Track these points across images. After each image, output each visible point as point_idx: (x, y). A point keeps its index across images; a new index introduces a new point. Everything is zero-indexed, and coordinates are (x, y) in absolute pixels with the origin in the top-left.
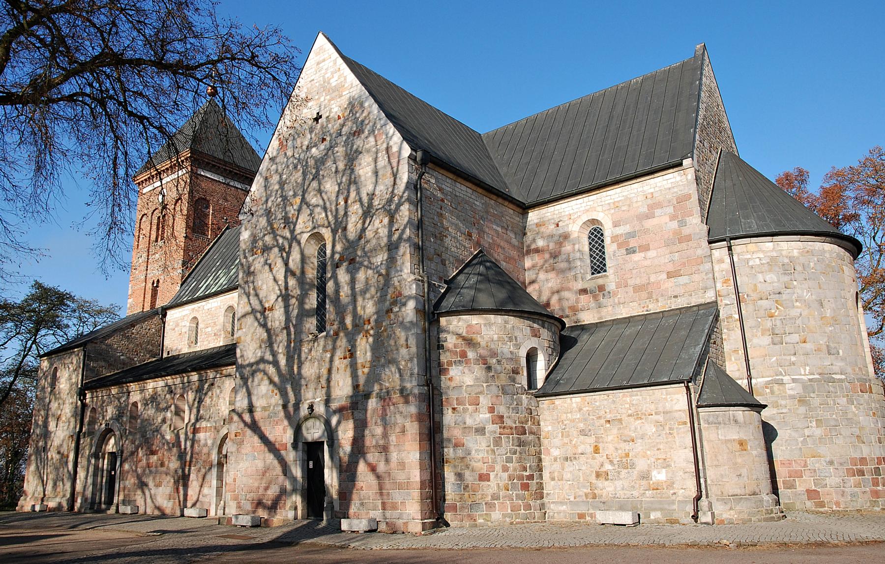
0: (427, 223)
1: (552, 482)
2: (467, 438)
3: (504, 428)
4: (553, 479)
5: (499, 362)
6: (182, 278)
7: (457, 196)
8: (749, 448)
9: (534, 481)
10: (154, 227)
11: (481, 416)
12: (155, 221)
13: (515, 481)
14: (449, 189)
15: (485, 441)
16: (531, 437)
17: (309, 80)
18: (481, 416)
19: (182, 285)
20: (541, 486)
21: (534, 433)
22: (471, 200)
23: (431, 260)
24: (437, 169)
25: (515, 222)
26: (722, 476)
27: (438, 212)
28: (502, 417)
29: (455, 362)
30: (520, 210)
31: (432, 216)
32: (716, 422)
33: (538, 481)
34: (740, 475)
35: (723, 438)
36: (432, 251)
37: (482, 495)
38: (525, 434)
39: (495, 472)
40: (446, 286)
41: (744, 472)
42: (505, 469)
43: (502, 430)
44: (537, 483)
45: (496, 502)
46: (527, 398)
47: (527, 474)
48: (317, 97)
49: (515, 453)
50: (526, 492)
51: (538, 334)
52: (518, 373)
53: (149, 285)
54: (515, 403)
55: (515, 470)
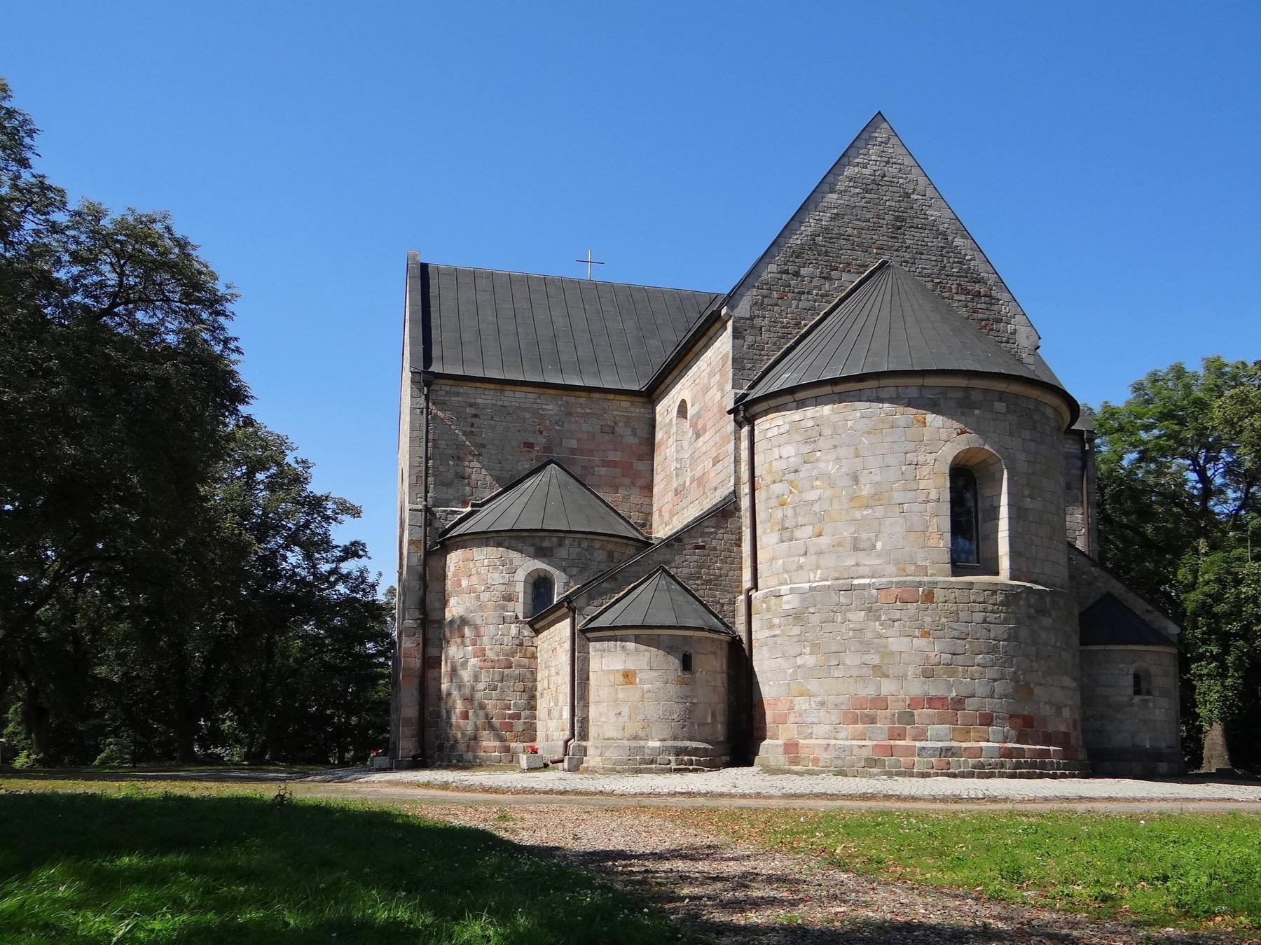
21: (524, 667)
30: (644, 400)
44: (525, 723)
47: (511, 712)
49: (495, 688)
52: (510, 599)
54: (500, 633)
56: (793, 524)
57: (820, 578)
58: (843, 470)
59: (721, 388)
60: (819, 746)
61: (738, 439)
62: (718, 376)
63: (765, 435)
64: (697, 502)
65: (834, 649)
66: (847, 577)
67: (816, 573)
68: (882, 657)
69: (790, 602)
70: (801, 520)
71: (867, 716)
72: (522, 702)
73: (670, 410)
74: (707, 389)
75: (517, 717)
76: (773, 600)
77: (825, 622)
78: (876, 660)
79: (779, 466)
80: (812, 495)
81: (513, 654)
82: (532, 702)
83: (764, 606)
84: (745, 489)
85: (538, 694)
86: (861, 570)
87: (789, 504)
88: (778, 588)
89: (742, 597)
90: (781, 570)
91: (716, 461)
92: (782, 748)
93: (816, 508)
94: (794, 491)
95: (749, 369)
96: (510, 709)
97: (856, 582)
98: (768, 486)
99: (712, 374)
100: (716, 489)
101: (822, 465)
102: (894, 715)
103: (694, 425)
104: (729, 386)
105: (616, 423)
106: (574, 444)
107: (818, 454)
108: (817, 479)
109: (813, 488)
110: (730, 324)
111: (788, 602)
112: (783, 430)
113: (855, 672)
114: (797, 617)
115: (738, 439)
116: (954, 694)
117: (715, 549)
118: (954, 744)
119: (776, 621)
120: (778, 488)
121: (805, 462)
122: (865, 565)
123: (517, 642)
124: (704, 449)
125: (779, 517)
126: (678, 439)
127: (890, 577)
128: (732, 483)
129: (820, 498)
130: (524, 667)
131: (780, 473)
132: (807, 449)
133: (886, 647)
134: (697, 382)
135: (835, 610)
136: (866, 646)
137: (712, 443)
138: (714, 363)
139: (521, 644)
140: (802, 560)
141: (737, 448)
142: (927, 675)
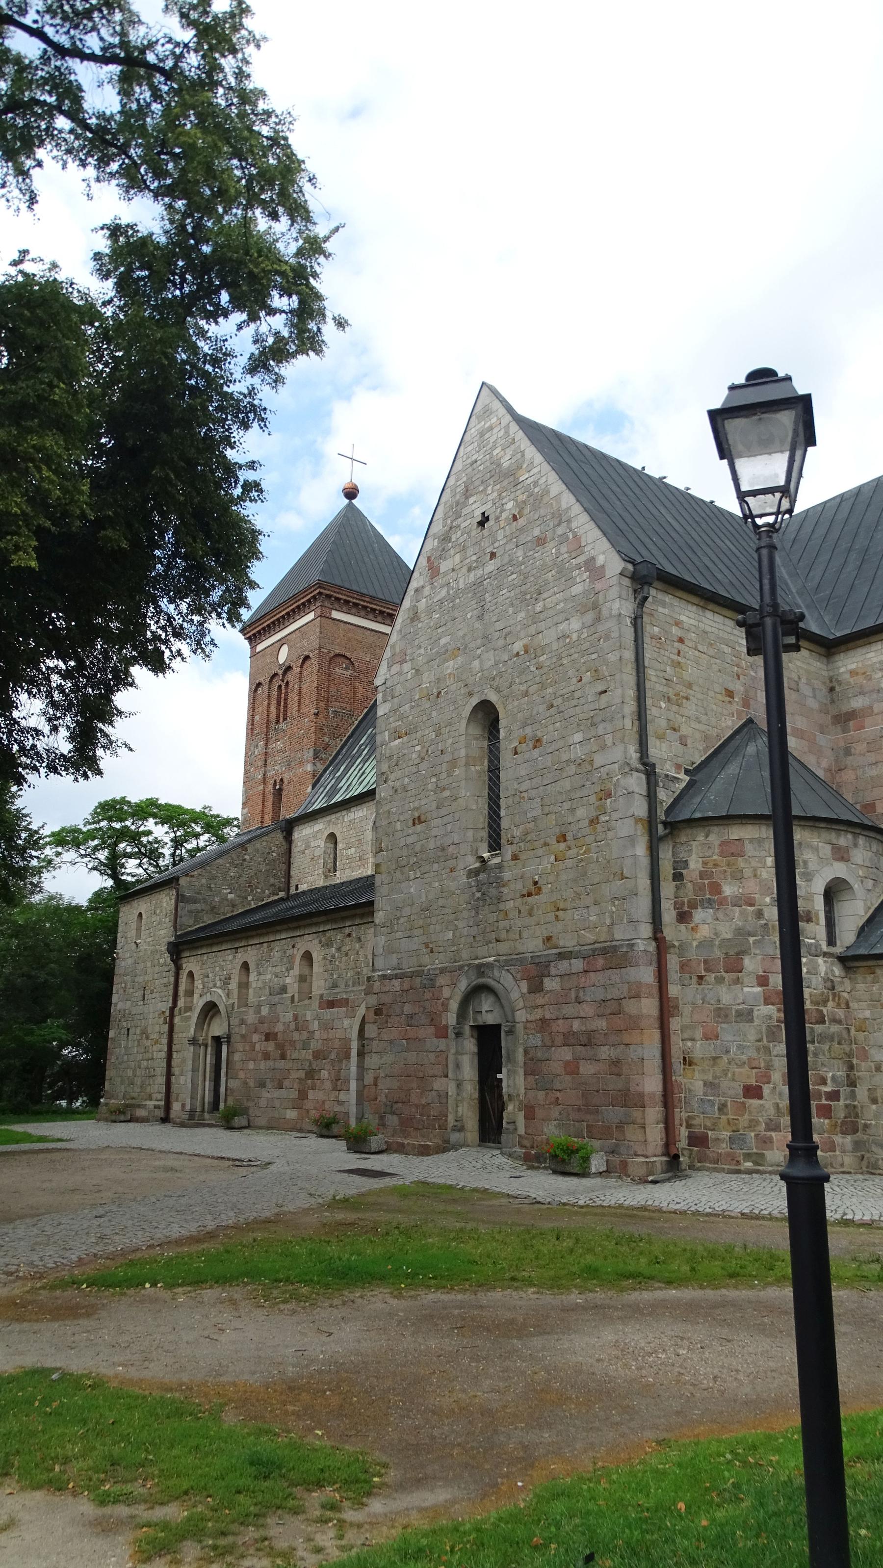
0: (653, 679)
1: (874, 1107)
2: (723, 1025)
4: (874, 1101)
6: (314, 776)
7: (707, 633)
9: (842, 1102)
10: (274, 702)
11: (745, 989)
12: (275, 693)
14: (692, 622)
15: (753, 1031)
16: (835, 1028)
17: (469, 461)
19: (313, 788)
20: (853, 1111)
21: (839, 1022)
22: (732, 638)
23: (661, 737)
24: (671, 589)
25: (813, 669)
27: (673, 661)
29: (702, 901)
30: (822, 650)
31: (662, 667)
33: (848, 1102)
36: (663, 723)
37: (751, 1121)
38: (823, 1022)
40: (687, 778)
44: (847, 1106)
45: (773, 1134)
46: (825, 962)
47: (828, 1089)
48: (481, 488)
50: (827, 1121)
51: (845, 856)
53: (270, 787)
72: (841, 1074)
81: (825, 1002)
123: (829, 984)
130: (839, 1022)
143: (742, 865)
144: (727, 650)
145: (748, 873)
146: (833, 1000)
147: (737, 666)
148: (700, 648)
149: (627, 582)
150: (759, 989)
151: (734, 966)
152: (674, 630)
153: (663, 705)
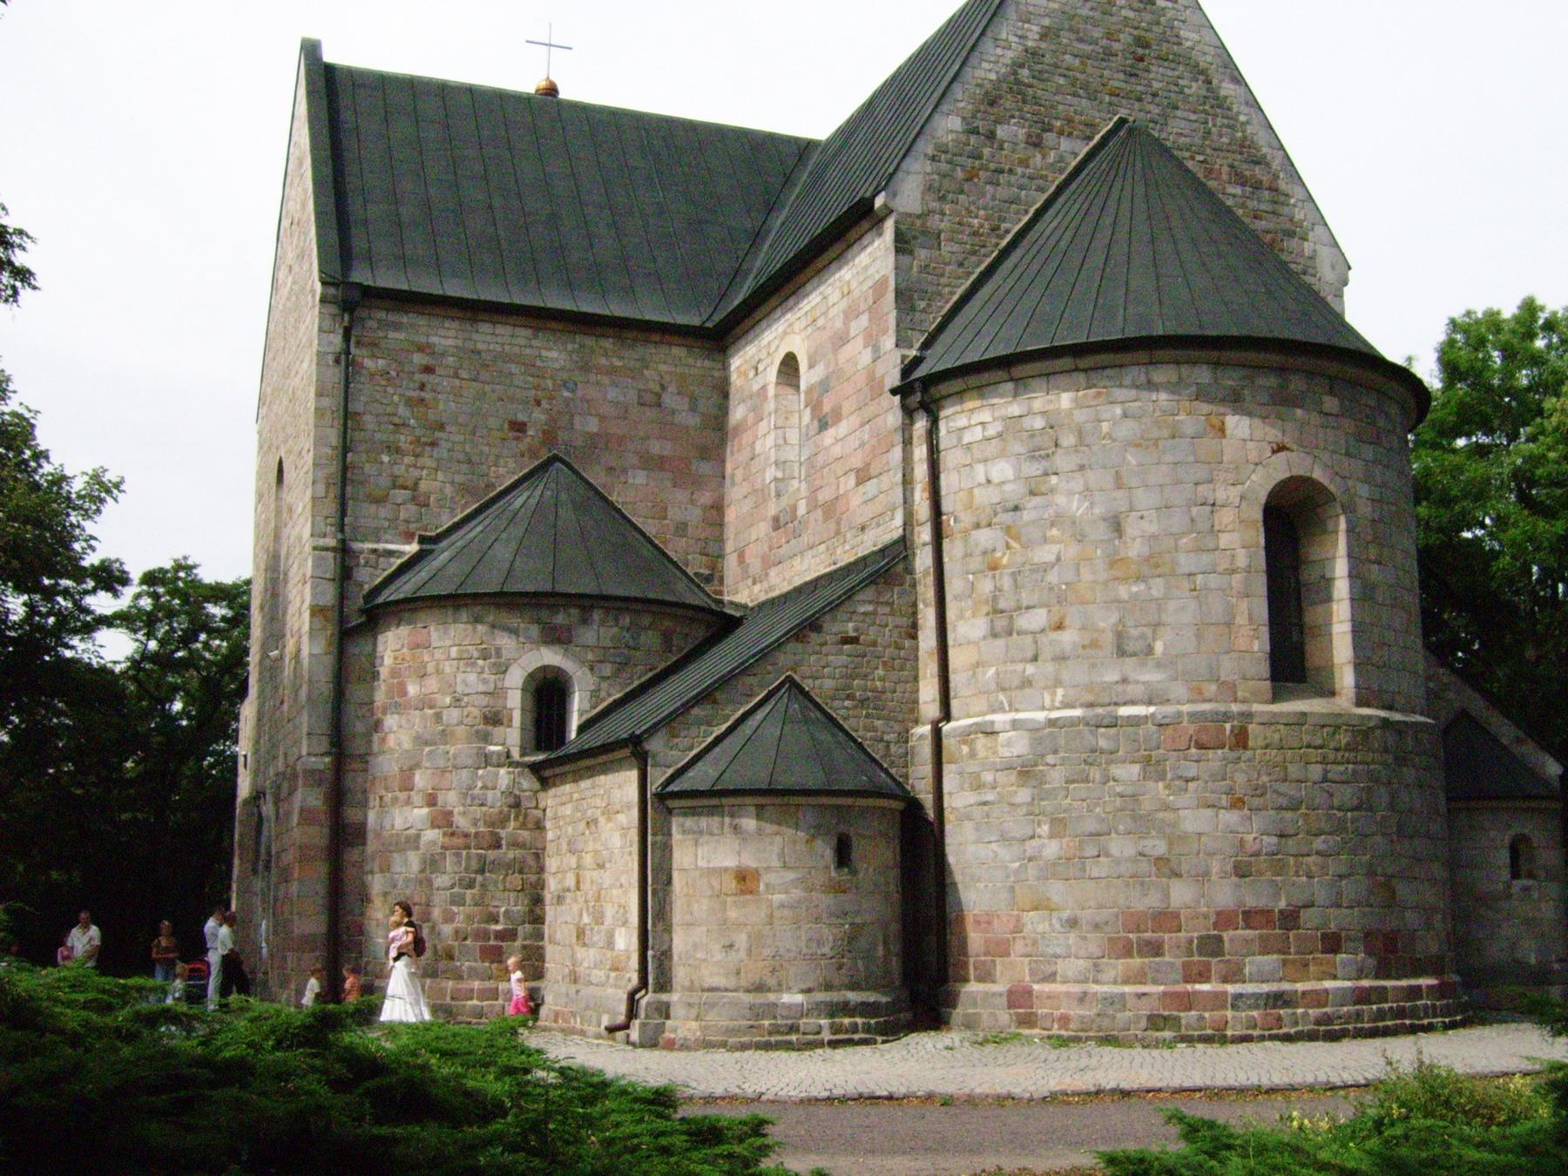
3: (453, 834)
5: (457, 701)
7: (479, 352)
8: (762, 887)
9: (518, 943)
13: (468, 942)
14: (450, 342)
18: (416, 811)
21: (522, 846)
23: (379, 501)
26: (695, 946)
28: (451, 813)
32: (696, 829)
34: (731, 946)
35: (705, 865)
38: (499, 846)
39: (430, 924)
41: (741, 939)
42: (449, 918)
43: (447, 839)
44: (524, 947)
47: (499, 927)
49: (471, 885)
50: (494, 966)
54: (480, 784)
55: (470, 918)
56: (1013, 604)
57: (1062, 702)
58: (1097, 511)
59: (872, 341)
60: (1068, 994)
61: (907, 442)
62: (864, 320)
63: (960, 439)
64: (822, 547)
65: (1091, 826)
66: (1107, 700)
67: (1054, 694)
68: (1171, 844)
69: (1014, 746)
70: (1026, 599)
71: (1148, 943)
72: (520, 909)
73: (761, 367)
74: (841, 340)
75: (509, 935)
76: (981, 742)
77: (1073, 782)
78: (1158, 847)
79: (984, 497)
80: (1046, 554)
81: (503, 821)
82: (537, 910)
83: (965, 749)
84: (924, 535)
85: (548, 897)
86: (1134, 690)
87: (1005, 567)
88: (989, 717)
89: (926, 729)
90: (993, 687)
91: (863, 476)
92: (1005, 999)
93: (1053, 577)
94: (1013, 544)
95: (924, 311)
96: (497, 922)
97: (1124, 711)
98: (966, 532)
99: (851, 314)
100: (863, 529)
101: (1061, 500)
102: (1190, 941)
103: (815, 406)
104: (888, 342)
105: (663, 387)
106: (593, 425)
107: (1054, 480)
108: (1052, 525)
109: (1045, 540)
110: (889, 225)
111: (1009, 744)
112: (991, 432)
113: (1124, 868)
114: (1026, 772)
115: (907, 442)
116: (1282, 904)
117: (874, 644)
118: (1286, 986)
119: (988, 777)
120: (984, 537)
121: (1032, 493)
122: (1137, 682)
123: (511, 800)
124: (837, 451)
125: (987, 591)
126: (780, 424)
127: (1178, 703)
128: (899, 520)
129: (1058, 559)
130: (522, 846)
131: (988, 510)
132: (1034, 469)
133: (1174, 825)
134: (820, 322)
135: (1090, 760)
136: (1142, 824)
137: (853, 442)
138: (856, 293)
139: (517, 805)
140: (1030, 669)
141: (907, 460)
142: (1241, 871)
143: (426, 658)
144: (513, 368)
145: (430, 668)
146: (517, 817)
147: (537, 388)
148: (464, 375)
149: (334, 309)
150: (425, 811)
151: (407, 786)
152: (419, 359)
153: (386, 459)
